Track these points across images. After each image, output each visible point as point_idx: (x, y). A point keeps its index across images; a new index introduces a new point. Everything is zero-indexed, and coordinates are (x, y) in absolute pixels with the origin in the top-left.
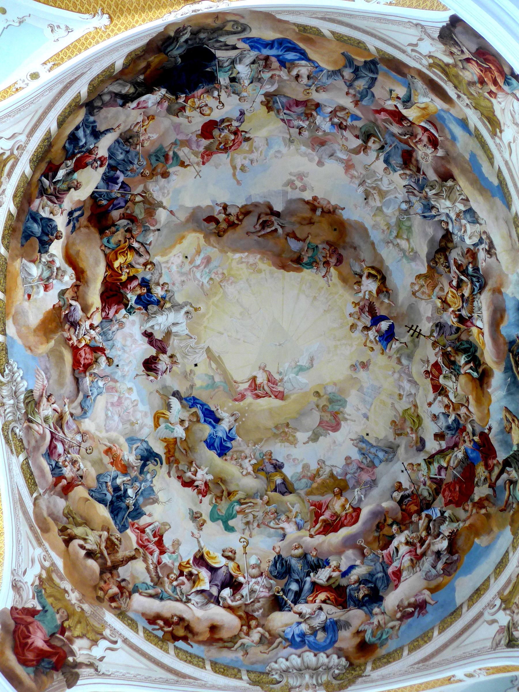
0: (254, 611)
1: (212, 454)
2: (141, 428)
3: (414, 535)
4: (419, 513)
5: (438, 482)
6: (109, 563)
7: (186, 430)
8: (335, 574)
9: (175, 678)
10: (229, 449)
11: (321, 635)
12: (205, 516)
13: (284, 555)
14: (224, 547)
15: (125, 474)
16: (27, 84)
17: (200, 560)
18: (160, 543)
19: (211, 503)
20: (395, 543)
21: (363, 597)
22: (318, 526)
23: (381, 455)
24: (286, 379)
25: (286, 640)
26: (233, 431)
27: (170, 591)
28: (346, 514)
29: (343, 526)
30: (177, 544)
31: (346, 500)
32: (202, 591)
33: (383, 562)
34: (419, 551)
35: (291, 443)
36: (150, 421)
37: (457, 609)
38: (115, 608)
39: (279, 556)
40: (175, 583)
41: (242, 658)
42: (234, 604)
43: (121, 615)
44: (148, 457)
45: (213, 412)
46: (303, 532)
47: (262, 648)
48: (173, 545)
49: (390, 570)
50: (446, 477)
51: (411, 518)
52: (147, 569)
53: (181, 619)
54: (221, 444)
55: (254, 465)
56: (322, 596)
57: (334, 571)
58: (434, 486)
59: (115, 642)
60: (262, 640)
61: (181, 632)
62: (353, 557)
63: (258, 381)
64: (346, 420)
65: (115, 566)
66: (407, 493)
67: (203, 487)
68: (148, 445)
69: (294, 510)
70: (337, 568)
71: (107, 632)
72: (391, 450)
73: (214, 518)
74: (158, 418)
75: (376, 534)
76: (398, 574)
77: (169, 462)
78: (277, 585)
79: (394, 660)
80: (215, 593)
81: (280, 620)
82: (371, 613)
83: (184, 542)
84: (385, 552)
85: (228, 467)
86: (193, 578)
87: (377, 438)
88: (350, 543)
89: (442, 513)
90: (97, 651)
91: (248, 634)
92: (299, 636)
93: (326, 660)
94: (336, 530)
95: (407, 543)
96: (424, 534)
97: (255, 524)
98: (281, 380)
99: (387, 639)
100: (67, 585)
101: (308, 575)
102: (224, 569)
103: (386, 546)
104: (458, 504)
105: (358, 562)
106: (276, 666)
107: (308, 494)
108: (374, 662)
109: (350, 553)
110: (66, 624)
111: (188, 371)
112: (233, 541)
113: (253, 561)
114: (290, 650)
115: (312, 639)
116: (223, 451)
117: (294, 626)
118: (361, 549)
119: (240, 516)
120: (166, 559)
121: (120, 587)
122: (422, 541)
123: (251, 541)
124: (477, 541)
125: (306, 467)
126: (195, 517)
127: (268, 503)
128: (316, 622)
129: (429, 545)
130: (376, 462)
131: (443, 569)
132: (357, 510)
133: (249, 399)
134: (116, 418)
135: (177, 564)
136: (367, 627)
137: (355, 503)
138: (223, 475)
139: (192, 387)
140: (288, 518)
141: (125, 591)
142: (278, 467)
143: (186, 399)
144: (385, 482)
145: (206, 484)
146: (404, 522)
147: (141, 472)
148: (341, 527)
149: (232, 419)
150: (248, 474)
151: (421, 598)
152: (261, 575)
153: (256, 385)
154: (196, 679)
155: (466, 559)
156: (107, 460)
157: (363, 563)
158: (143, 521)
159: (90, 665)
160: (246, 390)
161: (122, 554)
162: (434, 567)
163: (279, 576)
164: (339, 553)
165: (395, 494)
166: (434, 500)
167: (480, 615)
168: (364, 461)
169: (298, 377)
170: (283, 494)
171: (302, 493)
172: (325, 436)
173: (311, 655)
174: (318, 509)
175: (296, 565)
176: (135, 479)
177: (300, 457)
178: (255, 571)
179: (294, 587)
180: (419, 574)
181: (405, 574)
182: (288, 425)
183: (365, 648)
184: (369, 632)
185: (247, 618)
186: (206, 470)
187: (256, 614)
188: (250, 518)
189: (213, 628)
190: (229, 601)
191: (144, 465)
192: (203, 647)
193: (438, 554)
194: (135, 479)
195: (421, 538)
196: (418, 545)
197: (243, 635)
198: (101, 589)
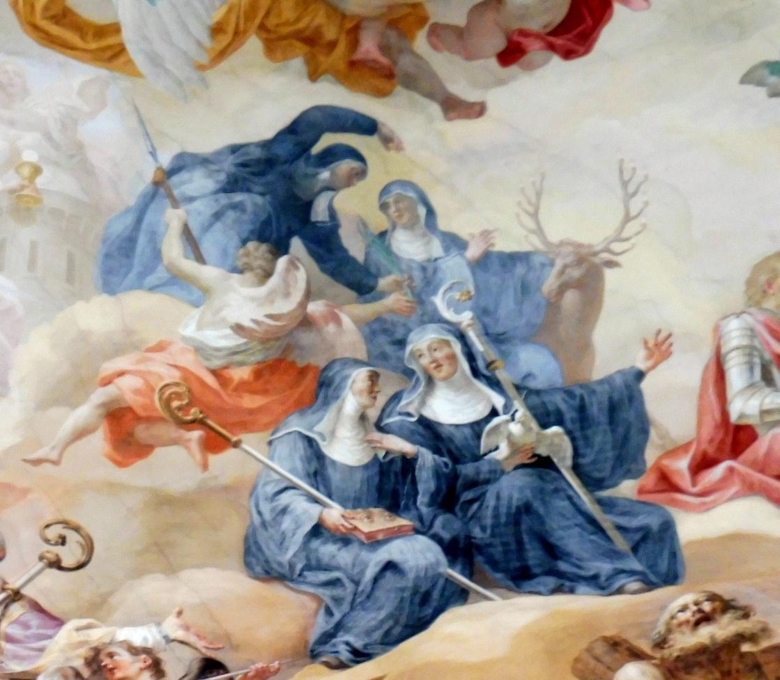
2: (76, 157)
15: (322, 388)
44: (281, 195)
68: (204, 161)
77: (383, 76)
147: (359, 281)
156: (175, 464)
176: (387, 342)
191: (325, 245)
194: (387, 342)
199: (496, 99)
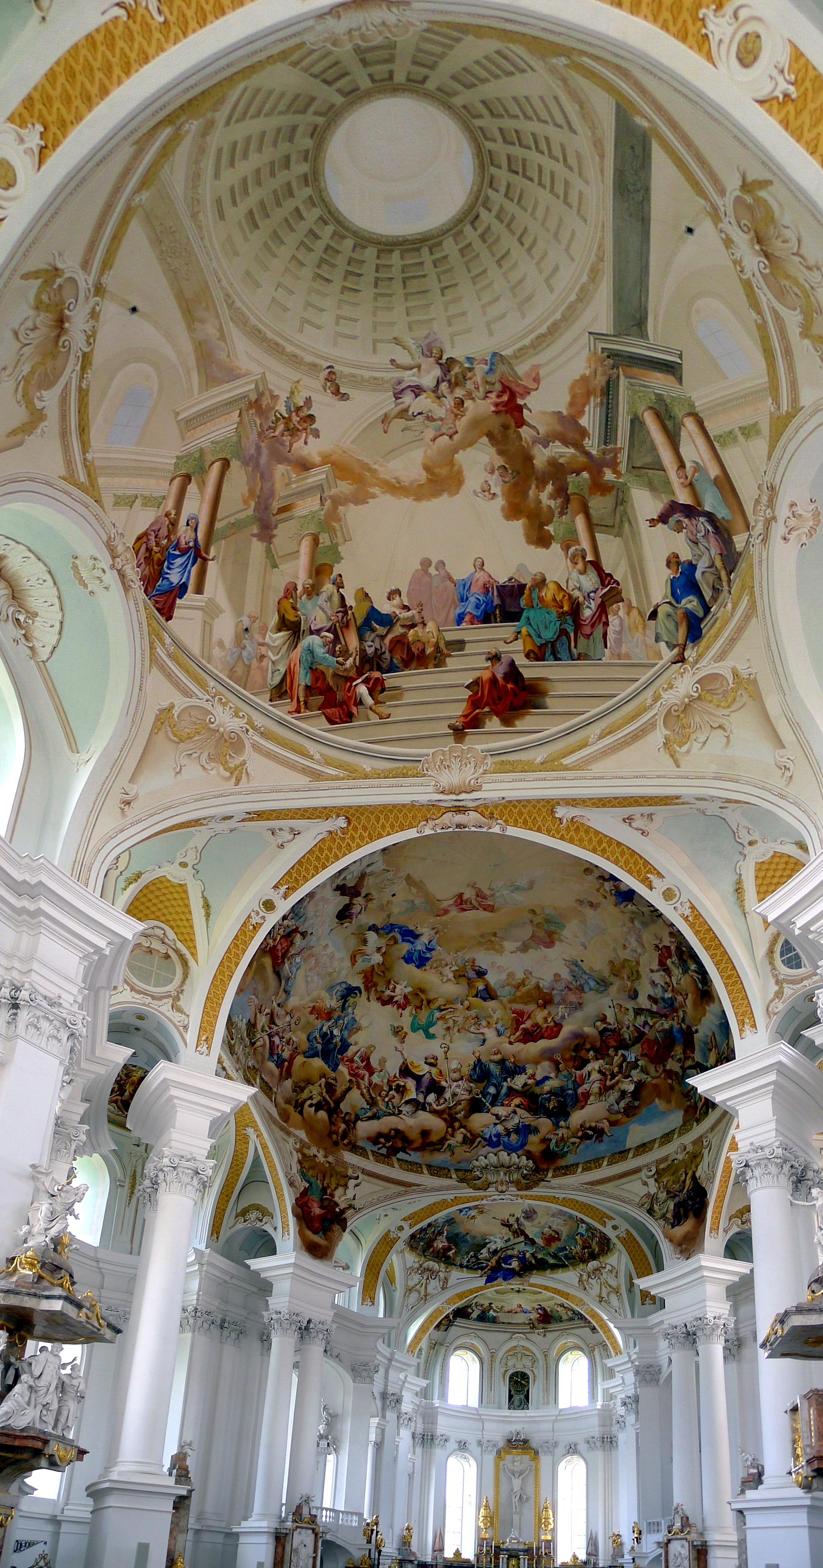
1: (412, 967)
2: (340, 972)
6: (332, 1105)
7: (384, 955)
8: (530, 1081)
10: (428, 959)
11: (514, 1137)
12: (407, 1029)
13: (483, 1060)
14: (426, 1055)
15: (329, 1019)
17: (406, 1071)
20: (589, 1067)
22: (518, 1033)
25: (485, 1139)
26: (433, 943)
27: (384, 1108)
29: (542, 1037)
30: (383, 1061)
33: (575, 1081)
34: (608, 1083)
35: (497, 951)
36: (347, 963)
39: (479, 1060)
42: (439, 1108)
44: (350, 992)
47: (465, 1148)
49: (580, 1091)
52: (362, 1094)
53: (397, 1131)
56: (517, 1101)
60: (466, 1141)
62: (548, 1069)
67: (402, 1001)
69: (495, 1017)
70: (533, 1076)
76: (587, 1095)
78: (476, 1088)
80: (422, 1101)
81: (480, 1121)
83: (388, 1059)
85: (428, 977)
86: (401, 1090)
88: (548, 1055)
91: (452, 1136)
92: (495, 1136)
95: (600, 1072)
96: (616, 1070)
97: (456, 1029)
102: (427, 1076)
103: (580, 1067)
105: (552, 1075)
107: (510, 1002)
109: (546, 1064)
111: (385, 902)
112: (435, 1048)
113: (454, 1065)
115: (506, 1139)
116: (421, 961)
118: (557, 1064)
119: (440, 1023)
120: (376, 1079)
122: (613, 1076)
123: (451, 1045)
124: (657, 1100)
125: (511, 975)
126: (397, 1031)
127: (468, 1009)
128: (510, 1125)
129: (618, 1082)
134: (315, 978)
135: (385, 1081)
138: (423, 986)
142: (481, 974)
143: (383, 929)
145: (405, 997)
146: (601, 1053)
151: (600, 1125)
152: (462, 1079)
155: (644, 1111)
161: (339, 1090)
163: (478, 1080)
164: (537, 1063)
170: (485, 999)
171: (505, 1000)
174: (519, 1017)
175: (495, 1069)
177: (504, 966)
178: (456, 1076)
179: (492, 1090)
181: (592, 1098)
186: (405, 984)
187: (458, 1116)
188: (451, 1023)
190: (434, 1106)
193: (623, 1093)
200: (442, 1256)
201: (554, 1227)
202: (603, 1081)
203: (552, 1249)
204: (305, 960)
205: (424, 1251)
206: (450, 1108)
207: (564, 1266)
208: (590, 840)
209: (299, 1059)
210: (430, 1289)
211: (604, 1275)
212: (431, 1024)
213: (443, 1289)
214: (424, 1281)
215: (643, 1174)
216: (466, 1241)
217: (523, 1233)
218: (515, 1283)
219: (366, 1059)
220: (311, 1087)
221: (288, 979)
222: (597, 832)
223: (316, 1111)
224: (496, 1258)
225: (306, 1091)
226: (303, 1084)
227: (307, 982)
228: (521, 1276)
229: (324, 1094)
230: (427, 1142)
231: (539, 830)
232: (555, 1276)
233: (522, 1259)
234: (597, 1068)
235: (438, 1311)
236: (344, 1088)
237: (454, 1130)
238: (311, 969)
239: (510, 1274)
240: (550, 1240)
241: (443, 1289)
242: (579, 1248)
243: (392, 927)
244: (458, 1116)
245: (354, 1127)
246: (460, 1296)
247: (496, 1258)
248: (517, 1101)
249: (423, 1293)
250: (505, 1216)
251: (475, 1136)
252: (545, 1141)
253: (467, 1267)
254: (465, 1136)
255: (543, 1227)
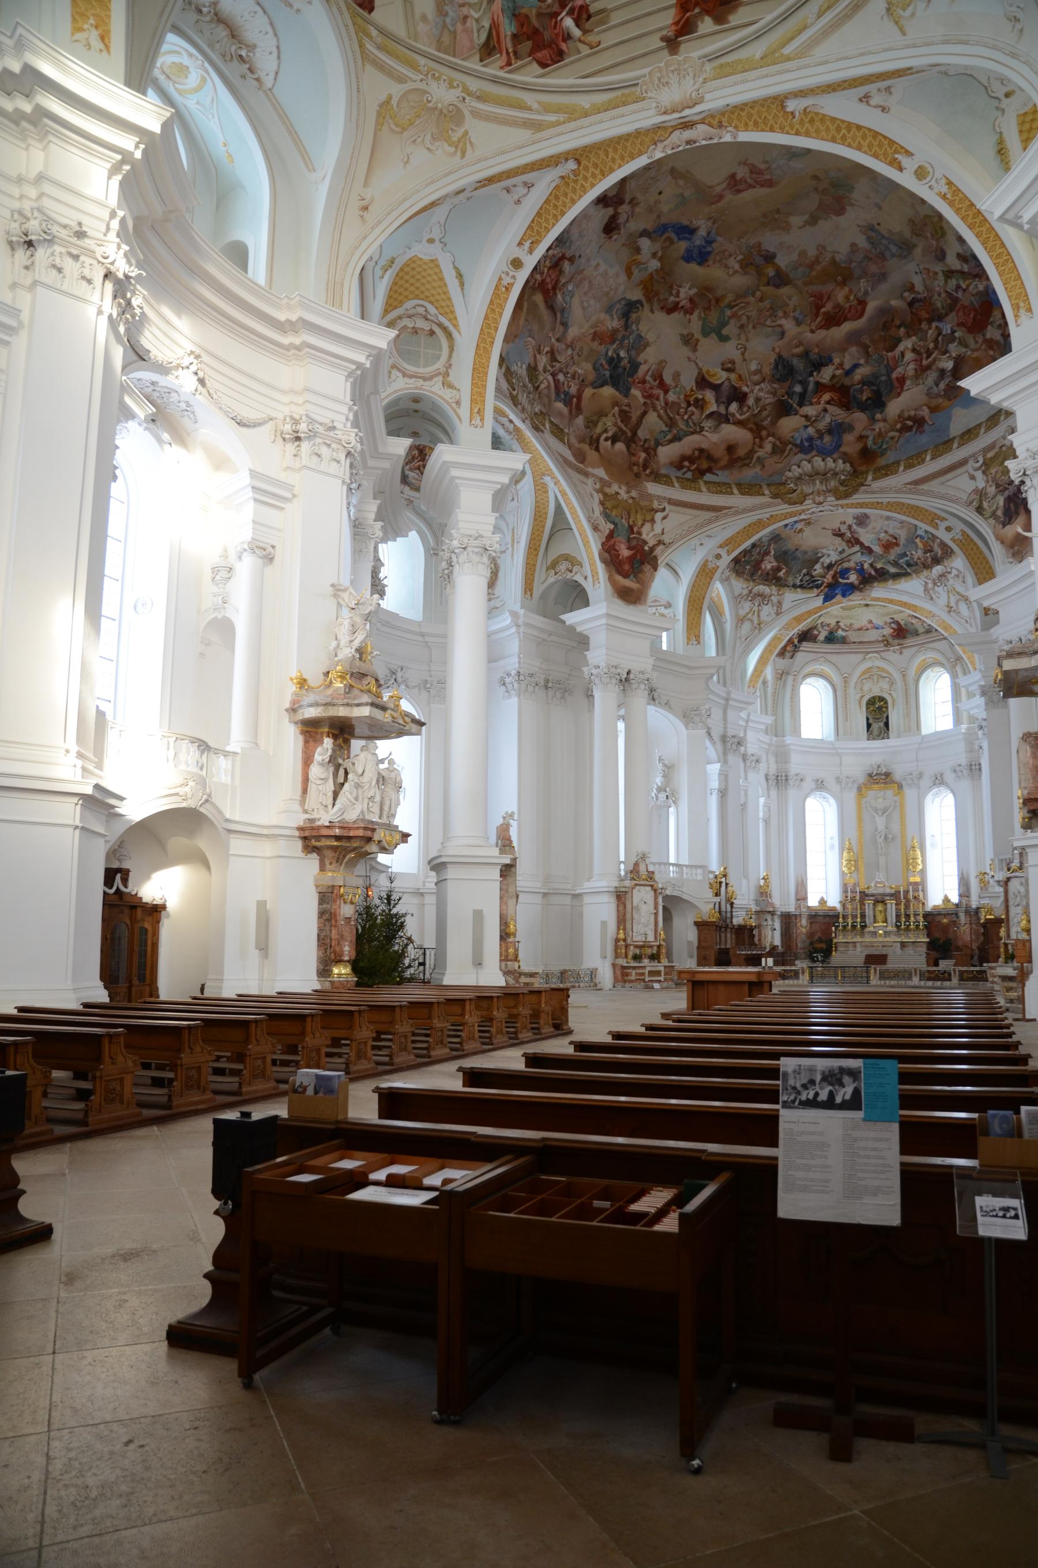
0: (762, 421)
1: (693, 266)
3: (922, 343)
4: (930, 321)
5: (955, 300)
6: (629, 434)
7: (660, 259)
8: (838, 372)
9: (714, 514)
10: (709, 253)
11: (827, 439)
13: (785, 354)
15: (612, 343)
16: (514, 277)
17: (703, 382)
18: (662, 385)
19: (700, 318)
20: (901, 347)
21: (867, 400)
22: (819, 319)
23: (894, 248)
24: (774, 166)
25: (796, 445)
26: (713, 234)
27: (684, 427)
28: (850, 307)
29: (846, 319)
30: (677, 376)
31: (851, 291)
32: (712, 414)
34: (925, 362)
36: (623, 277)
37: (949, 440)
38: (651, 473)
39: (780, 357)
40: (686, 417)
41: (760, 473)
42: (743, 417)
43: (657, 477)
44: (630, 308)
45: (686, 227)
46: (804, 328)
47: (775, 458)
48: (674, 379)
50: (964, 299)
51: (920, 324)
52: (660, 417)
53: (701, 451)
54: (700, 252)
55: (740, 262)
56: (826, 397)
57: (837, 369)
58: (949, 301)
59: (664, 509)
61: (705, 465)
63: (738, 177)
64: (852, 205)
65: (635, 433)
66: (919, 296)
67: (688, 305)
69: (792, 304)
71: (656, 505)
72: (906, 248)
73: (705, 333)
74: (630, 269)
75: (882, 333)
76: (902, 380)
78: (781, 389)
79: (892, 474)
81: (789, 425)
82: (873, 418)
84: (890, 354)
85: (713, 272)
86: (700, 404)
87: (890, 231)
88: (853, 338)
89: (953, 332)
90: (658, 529)
91: (761, 447)
92: (807, 440)
93: (833, 465)
94: (839, 324)
95: (914, 350)
96: (931, 346)
97: (750, 326)
98: (769, 168)
99: (886, 449)
100: (615, 488)
101: (811, 375)
102: (726, 383)
103: (892, 348)
104: (970, 330)
105: (862, 361)
106: (790, 474)
107: (805, 284)
108: (874, 472)
109: (853, 349)
110: (631, 523)
112: (731, 350)
113: (753, 367)
114: (800, 456)
115: (818, 442)
116: (701, 256)
117: (802, 430)
118: (865, 348)
119: (732, 322)
120: (672, 397)
121: (646, 450)
125: (803, 254)
126: (688, 340)
127: (761, 300)
128: (822, 425)
130: (887, 254)
131: (944, 390)
132: (862, 303)
133: (729, 197)
134: (592, 302)
135: (682, 397)
136: (869, 433)
137: (860, 295)
139: (659, 216)
140: (785, 313)
141: (651, 451)
142: (769, 258)
143: (654, 232)
144: (895, 279)
145: (691, 300)
146: (913, 327)
148: (844, 321)
149: (710, 223)
150: (736, 272)
152: (764, 380)
153: (735, 181)
154: (730, 508)
157: (867, 362)
158: (641, 373)
159: (660, 542)
160: (724, 190)
161: (635, 415)
162: (937, 385)
163: (781, 380)
164: (843, 350)
165: (906, 294)
166: (947, 315)
167: (963, 463)
168: (873, 250)
169: (791, 163)
170: (778, 287)
171: (799, 283)
172: (826, 219)
173: (819, 459)
174: (818, 302)
175: (798, 364)
177: (794, 243)
178: (757, 378)
179: (798, 389)
180: (921, 387)
181: (908, 382)
182: (778, 211)
183: (867, 455)
184: (871, 438)
185: (757, 428)
186: (688, 286)
187: (765, 423)
188: (744, 319)
189: (731, 448)
192: (726, 472)
193: (942, 372)
195: (928, 349)
196: (925, 355)
197: (757, 449)
198: (634, 464)
199: (656, 312)
200: (773, 578)
201: (891, 531)
202: (918, 361)
203: (892, 556)
204: (577, 286)
205: (752, 575)
206: (754, 416)
207: (906, 574)
208: (828, 129)
209: (588, 392)
210: (764, 616)
211: (951, 581)
212: (724, 324)
213: (777, 614)
214: (756, 608)
215: (971, 463)
216: (795, 558)
217: (858, 542)
218: (856, 599)
219: (659, 377)
220: (604, 419)
221: (563, 311)
222: (833, 119)
223: (613, 442)
224: (832, 573)
225: (600, 425)
226: (595, 418)
227: (584, 308)
228: (861, 590)
229: (620, 424)
230: (735, 457)
231: (772, 130)
232: (897, 587)
233: (861, 571)
234: (910, 346)
235: (776, 639)
236: (639, 413)
237: (761, 439)
238: (585, 294)
239: (850, 589)
240: (888, 546)
241: (777, 614)
242: (920, 552)
243: (664, 228)
244: (765, 423)
245: (656, 455)
246: (799, 619)
247: (832, 573)
248: (826, 397)
249: (756, 622)
250: (836, 525)
251: (785, 444)
252: (862, 438)
253: (801, 587)
254: (774, 445)
255: (879, 533)
